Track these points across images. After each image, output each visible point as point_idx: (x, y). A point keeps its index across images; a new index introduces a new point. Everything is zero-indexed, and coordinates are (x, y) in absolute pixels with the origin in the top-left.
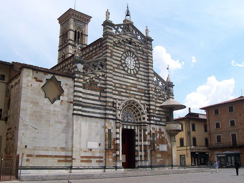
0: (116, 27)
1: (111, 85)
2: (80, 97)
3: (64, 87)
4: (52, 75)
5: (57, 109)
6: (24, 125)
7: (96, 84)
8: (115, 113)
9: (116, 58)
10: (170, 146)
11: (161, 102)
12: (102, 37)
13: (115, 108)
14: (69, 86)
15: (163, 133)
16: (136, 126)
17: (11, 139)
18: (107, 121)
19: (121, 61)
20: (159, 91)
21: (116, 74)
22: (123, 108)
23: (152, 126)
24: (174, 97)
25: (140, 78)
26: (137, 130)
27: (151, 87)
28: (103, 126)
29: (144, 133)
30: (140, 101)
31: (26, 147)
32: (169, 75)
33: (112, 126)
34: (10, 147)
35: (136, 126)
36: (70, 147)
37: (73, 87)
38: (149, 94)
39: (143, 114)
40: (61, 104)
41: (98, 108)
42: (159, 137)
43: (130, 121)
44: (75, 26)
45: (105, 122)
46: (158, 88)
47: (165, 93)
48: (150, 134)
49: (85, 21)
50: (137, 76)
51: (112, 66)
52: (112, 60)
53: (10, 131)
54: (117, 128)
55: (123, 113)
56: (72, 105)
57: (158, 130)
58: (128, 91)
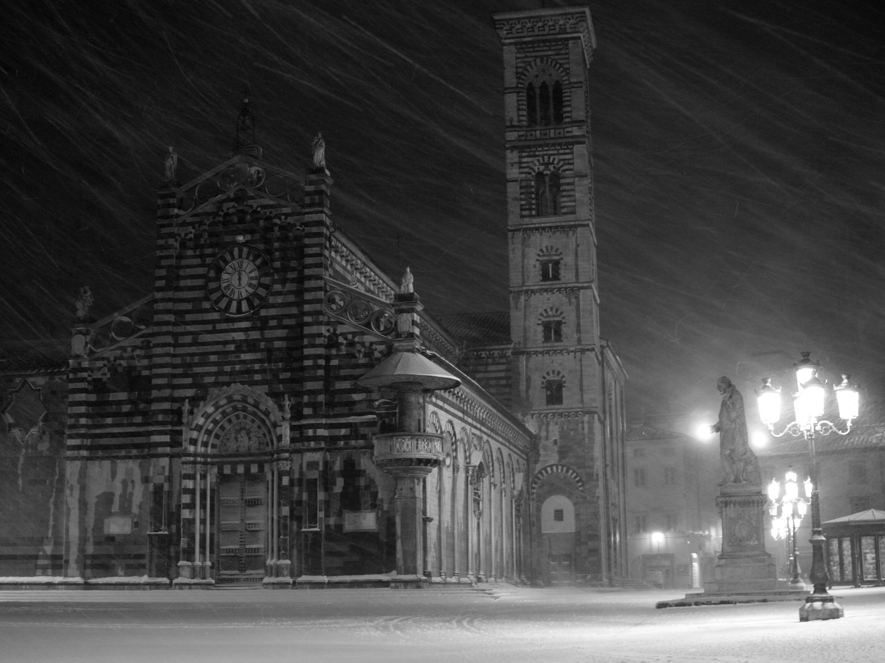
9: (189, 283)
16: (266, 462)
19: (203, 287)
20: (346, 339)
25: (273, 317)
35: (266, 462)
47: (374, 339)
50: (263, 313)
51: (168, 312)
52: (170, 294)
58: (228, 368)
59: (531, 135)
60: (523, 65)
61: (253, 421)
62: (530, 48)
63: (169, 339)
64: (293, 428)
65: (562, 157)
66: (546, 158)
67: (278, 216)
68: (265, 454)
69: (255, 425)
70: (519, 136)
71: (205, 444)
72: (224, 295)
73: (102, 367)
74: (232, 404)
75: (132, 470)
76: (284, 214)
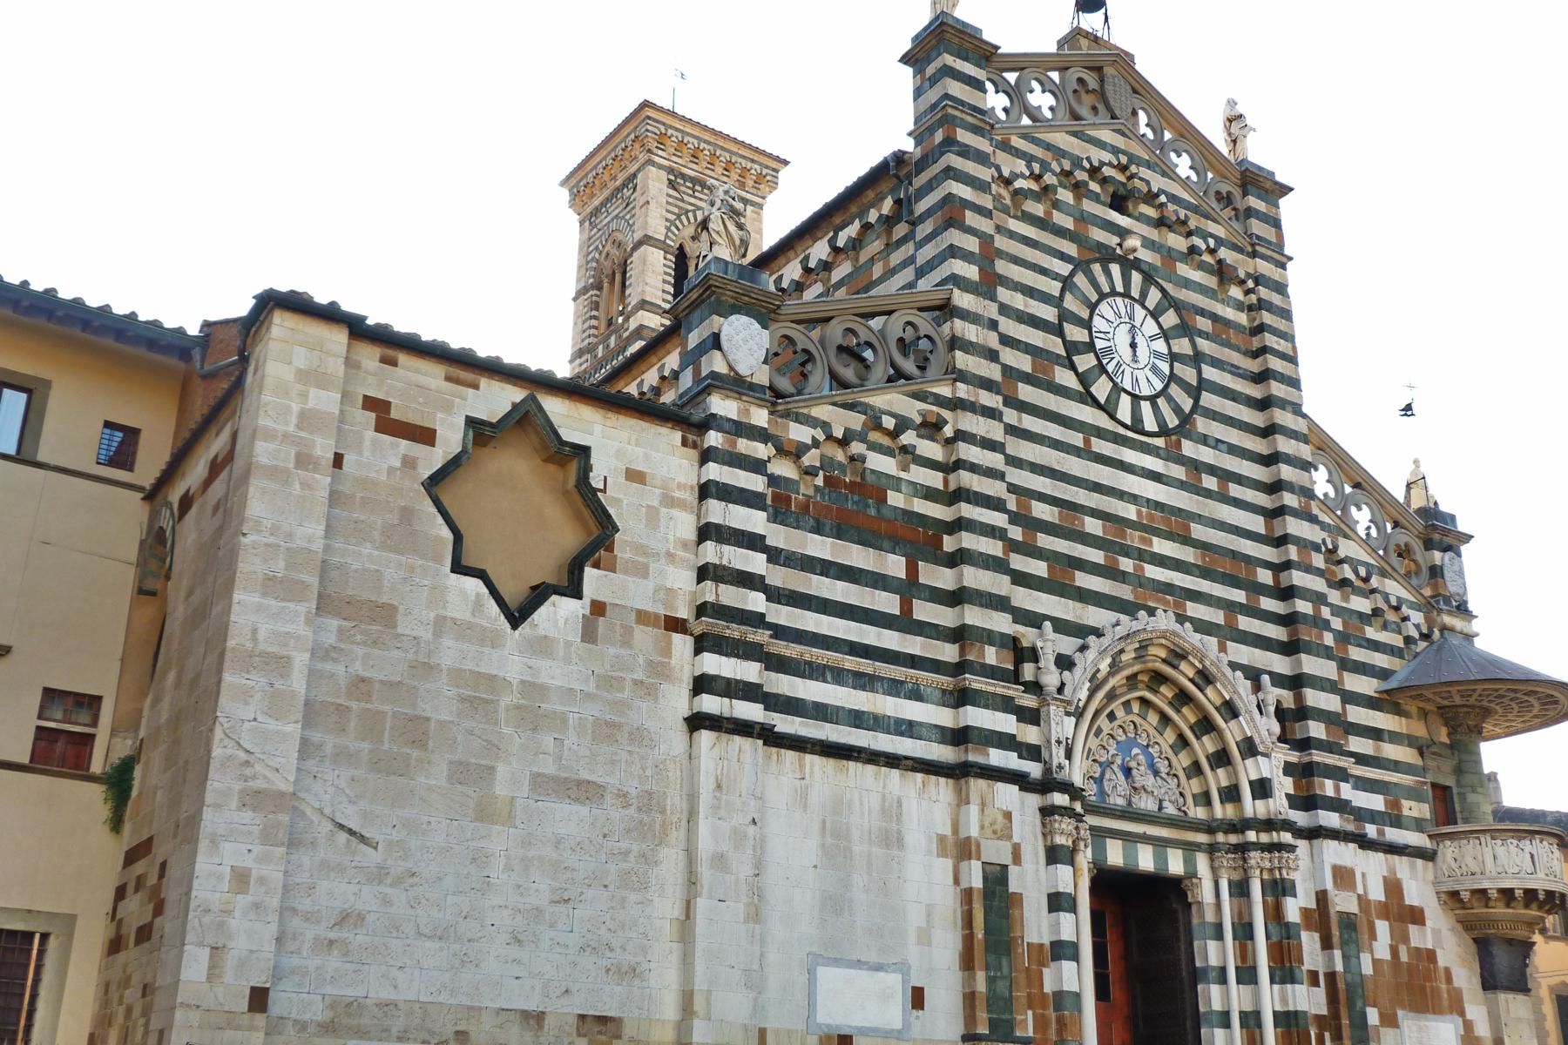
0: (1011, 77)
1: (995, 504)
2: (747, 580)
3: (621, 502)
4: (516, 394)
5: (553, 674)
6: (255, 799)
7: (872, 489)
8: (1031, 735)
9: (1018, 301)
10: (1483, 1030)
11: (1381, 660)
12: (908, 145)
13: (1035, 687)
14: (658, 491)
17: (144, 934)
18: (975, 798)
21: (1030, 423)
22: (1092, 693)
24: (1476, 626)
25: (1212, 470)
26: (1206, 893)
27: (1298, 541)
28: (942, 839)
29: (1275, 914)
30: (1223, 649)
31: (259, 999)
32: (1416, 462)
33: (1016, 839)
34: (129, 1010)
35: (1197, 847)
36: (669, 1010)
37: (691, 497)
38: (1287, 593)
39: (1249, 748)
40: (589, 634)
41: (895, 688)
42: (1394, 952)
43: (1147, 804)
44: (679, 217)
45: (962, 800)
46: (1346, 548)
47: (1405, 594)
48: (1320, 916)
49: (742, 186)
50: (1189, 448)
52: (991, 310)
53: (139, 868)
54: (1054, 855)
55: (1093, 743)
56: (682, 644)
57: (1377, 893)
58: (1127, 564)
60: (676, 211)
62: (689, 188)
67: (1205, 235)
68: (1196, 826)
72: (1102, 369)
73: (806, 448)
75: (899, 802)
76: (1212, 235)
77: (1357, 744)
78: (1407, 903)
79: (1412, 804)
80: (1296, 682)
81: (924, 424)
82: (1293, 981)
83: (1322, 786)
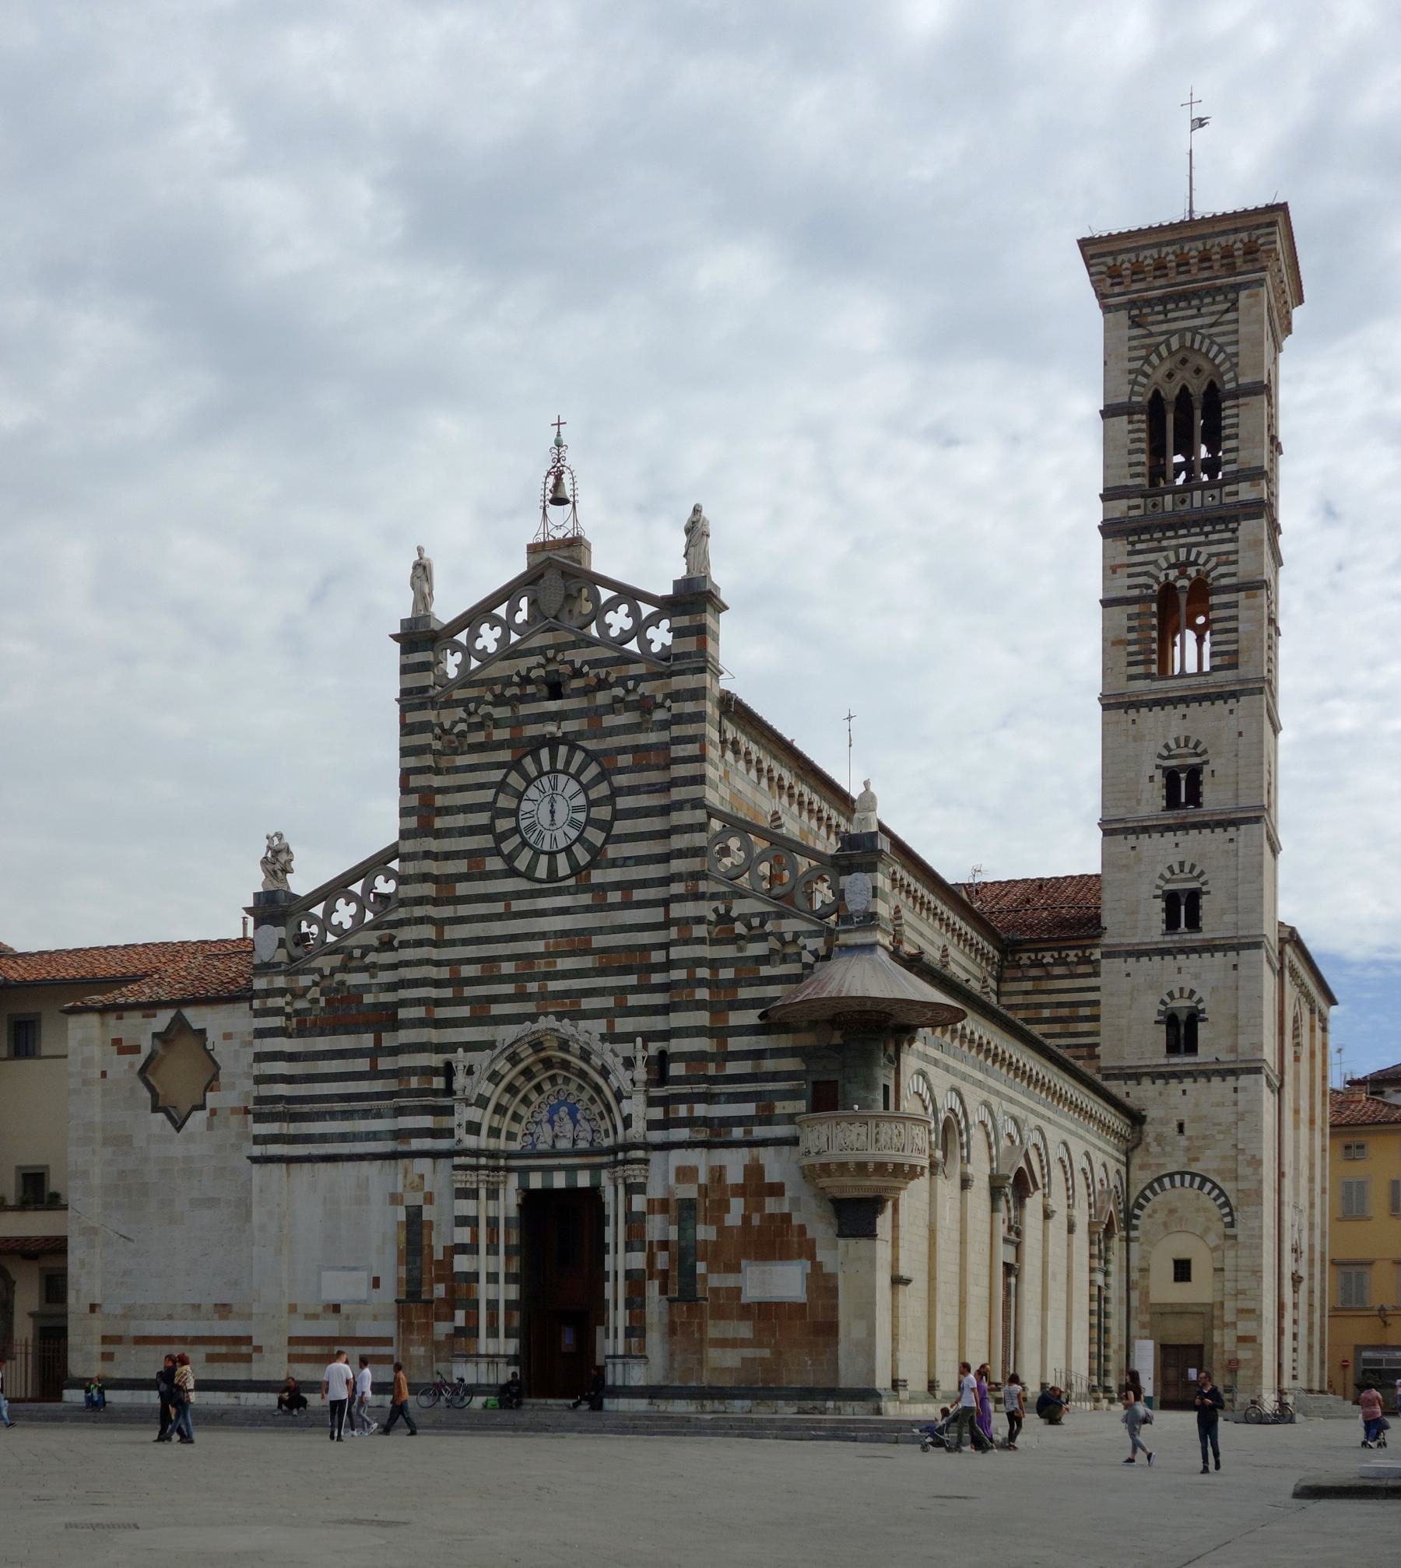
13: (449, 1091)
15: (777, 1190)
16: (602, 1166)
21: (464, 910)
23: (677, 1158)
30: (611, 1025)
35: (602, 1166)
39: (619, 1096)
42: (746, 1219)
57: (735, 1176)
58: (533, 987)
59: (1154, 505)
61: (581, 1088)
63: (428, 932)
64: (651, 1102)
65: (1214, 549)
66: (1183, 552)
69: (585, 1096)
70: (1130, 508)
71: (494, 1132)
74: (543, 1054)
77: (732, 1068)
78: (767, 1180)
79: (786, 1103)
80: (667, 1035)
81: (382, 944)
82: (632, 1250)
83: (676, 1111)
